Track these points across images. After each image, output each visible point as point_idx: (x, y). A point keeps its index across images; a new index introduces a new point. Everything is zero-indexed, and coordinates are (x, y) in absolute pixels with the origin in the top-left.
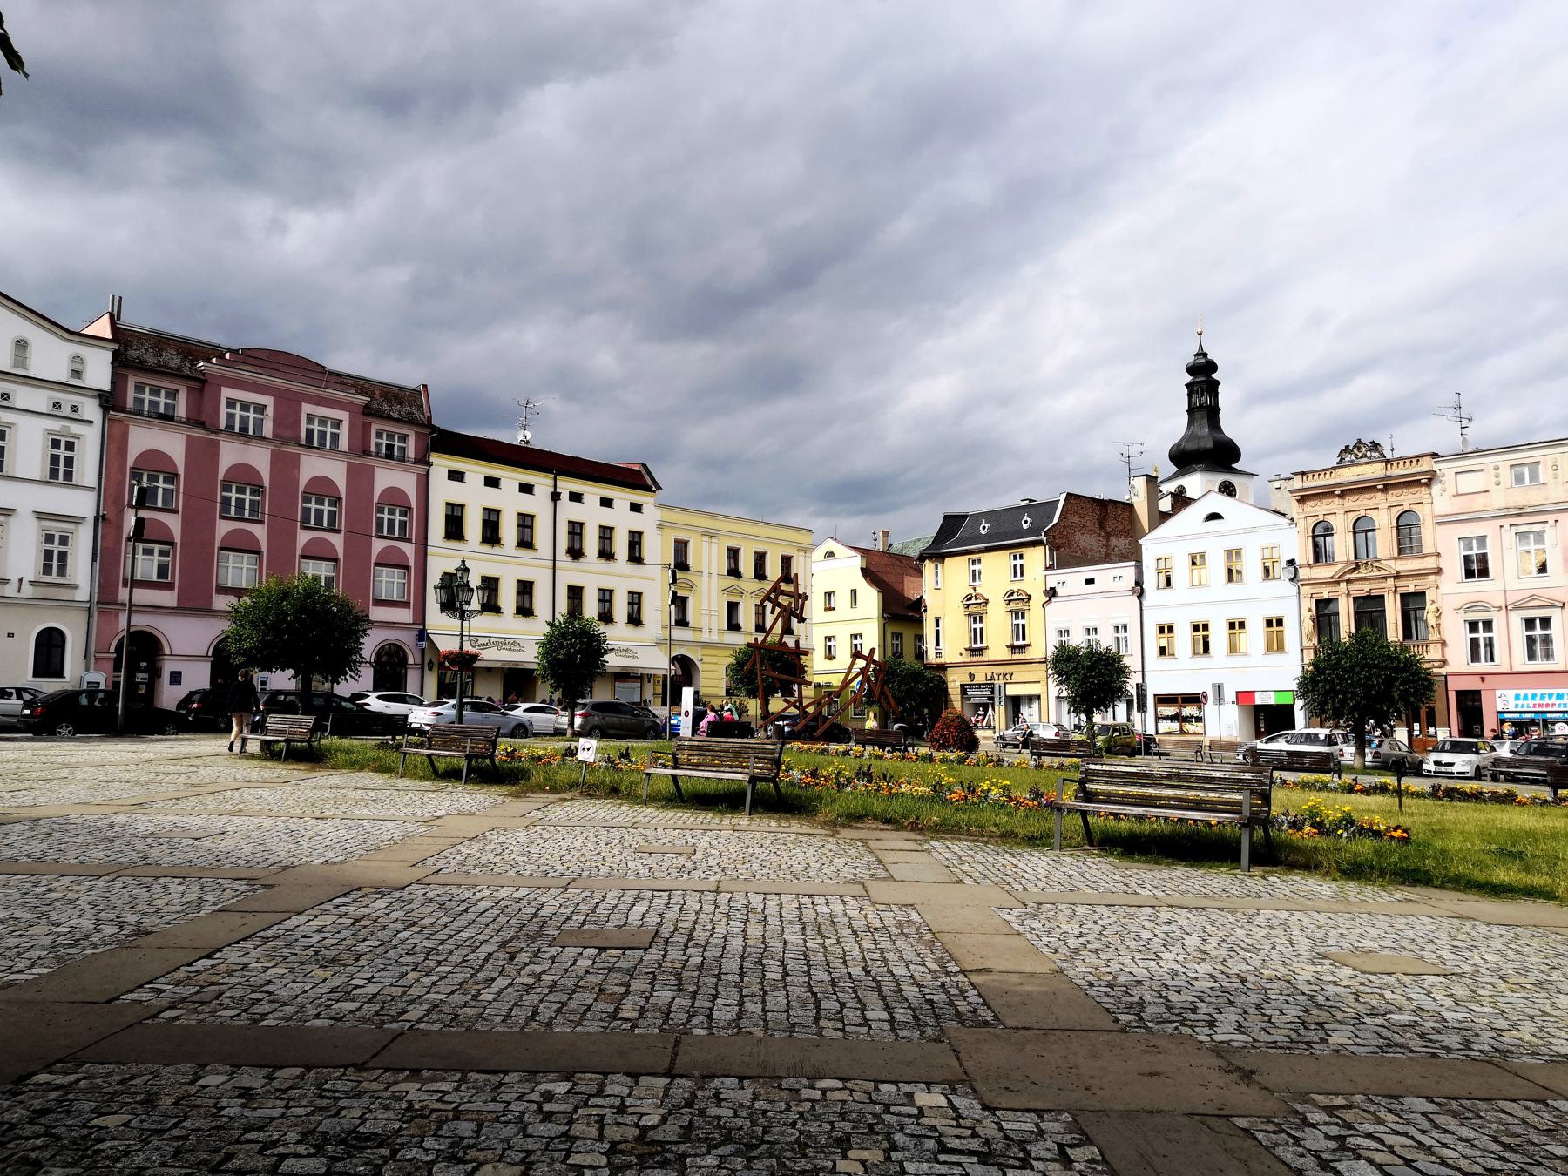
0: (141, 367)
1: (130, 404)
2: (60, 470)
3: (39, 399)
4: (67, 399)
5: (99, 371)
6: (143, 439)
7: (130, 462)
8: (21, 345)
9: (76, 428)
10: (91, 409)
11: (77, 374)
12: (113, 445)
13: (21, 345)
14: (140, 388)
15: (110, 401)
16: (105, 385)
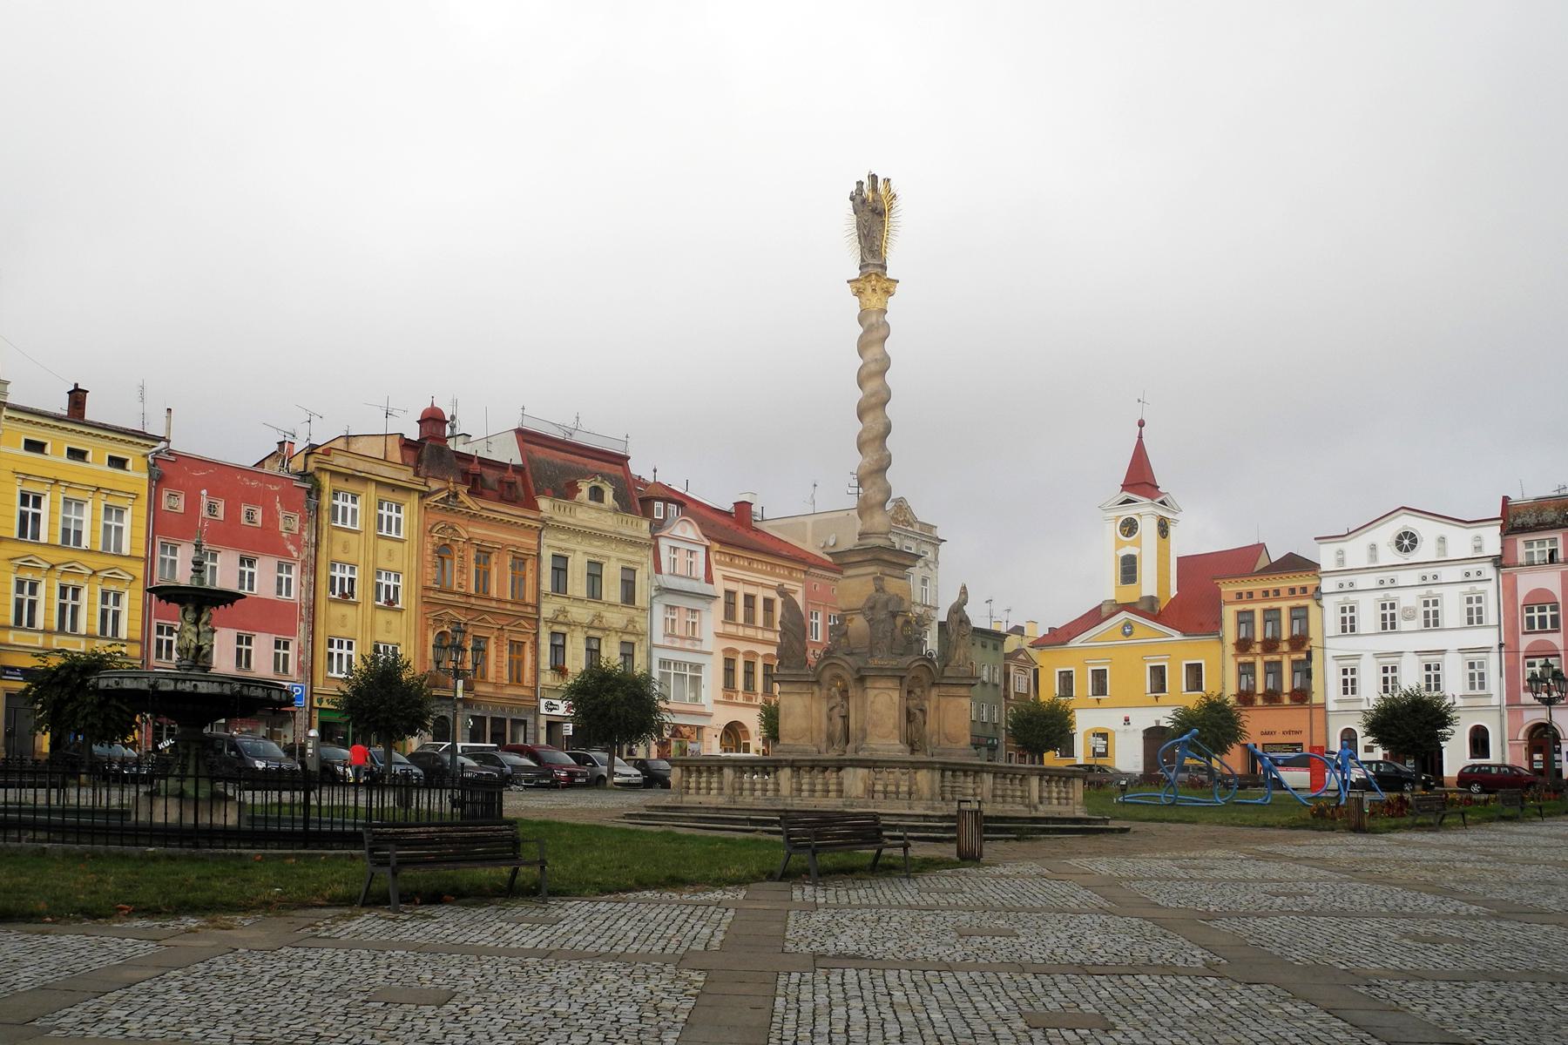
0: (1524, 529)
1: (1522, 559)
2: (1474, 618)
3: (1454, 573)
4: (1473, 568)
5: (1492, 540)
6: (1528, 583)
7: (1520, 602)
8: (1442, 540)
9: (1479, 587)
10: (1489, 571)
11: (1478, 548)
12: (1510, 590)
13: (1442, 540)
14: (1529, 544)
15: (1498, 562)
16: (1499, 552)
